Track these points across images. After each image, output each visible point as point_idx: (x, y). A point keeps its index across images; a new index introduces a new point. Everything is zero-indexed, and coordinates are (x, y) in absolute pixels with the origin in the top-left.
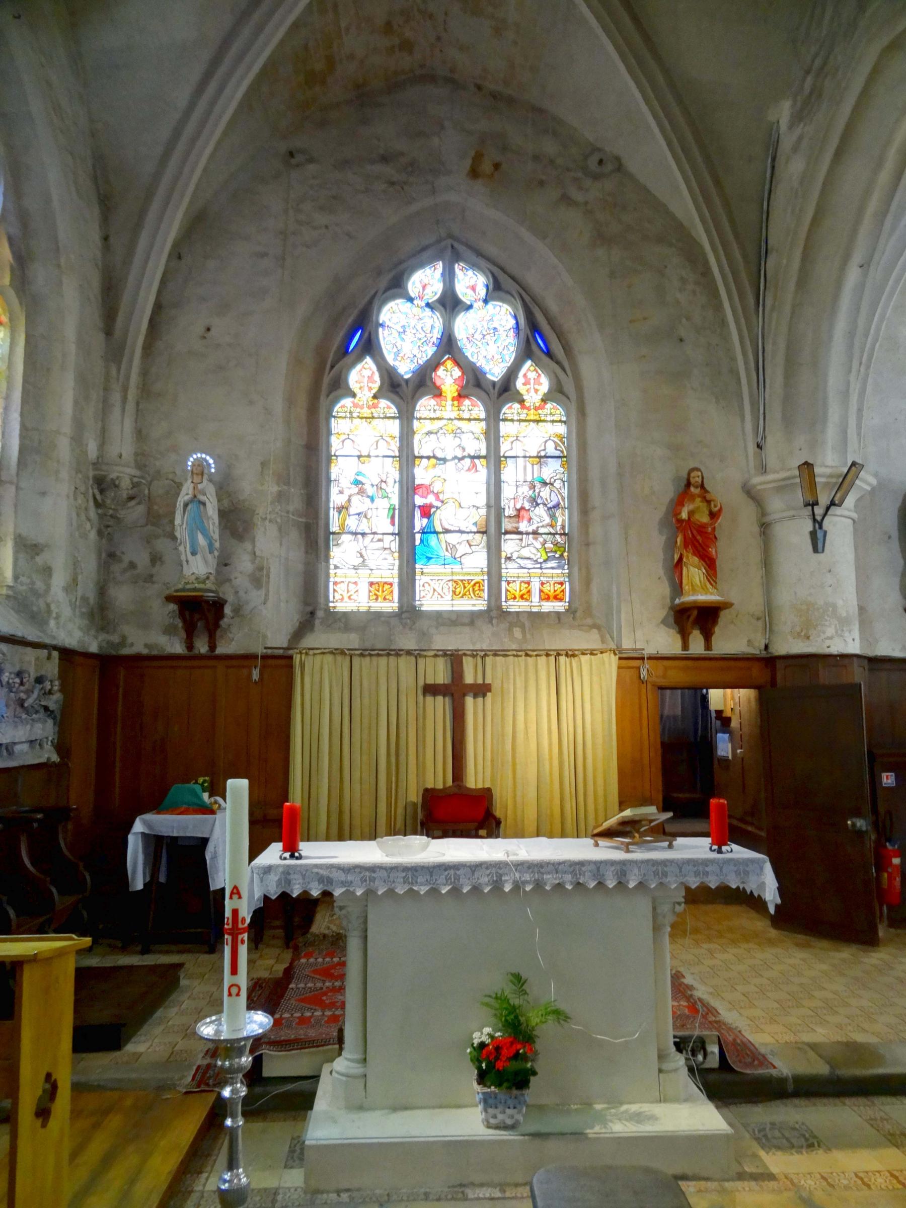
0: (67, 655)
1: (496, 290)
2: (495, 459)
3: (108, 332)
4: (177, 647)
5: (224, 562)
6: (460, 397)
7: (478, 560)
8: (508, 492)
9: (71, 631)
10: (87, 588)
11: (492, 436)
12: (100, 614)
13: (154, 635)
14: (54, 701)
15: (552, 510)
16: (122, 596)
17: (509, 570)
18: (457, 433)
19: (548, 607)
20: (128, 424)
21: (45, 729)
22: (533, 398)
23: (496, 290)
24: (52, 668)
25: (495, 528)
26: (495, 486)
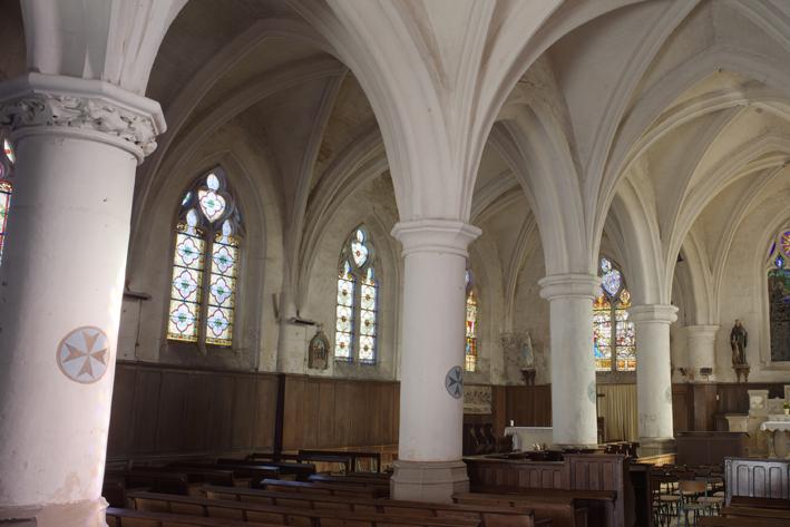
0: (494, 387)
1: (614, 267)
2: (614, 323)
3: (504, 296)
4: (523, 383)
5: (535, 360)
6: (603, 304)
7: (609, 355)
8: (618, 333)
9: (496, 380)
10: (502, 369)
11: (613, 315)
12: (505, 375)
13: (517, 380)
14: (490, 399)
15: (631, 338)
16: (510, 369)
17: (619, 358)
18: (602, 314)
19: (630, 369)
20: (511, 320)
21: (488, 406)
22: (626, 301)
23: (614, 267)
24: (490, 391)
25: (615, 344)
26: (614, 331)
